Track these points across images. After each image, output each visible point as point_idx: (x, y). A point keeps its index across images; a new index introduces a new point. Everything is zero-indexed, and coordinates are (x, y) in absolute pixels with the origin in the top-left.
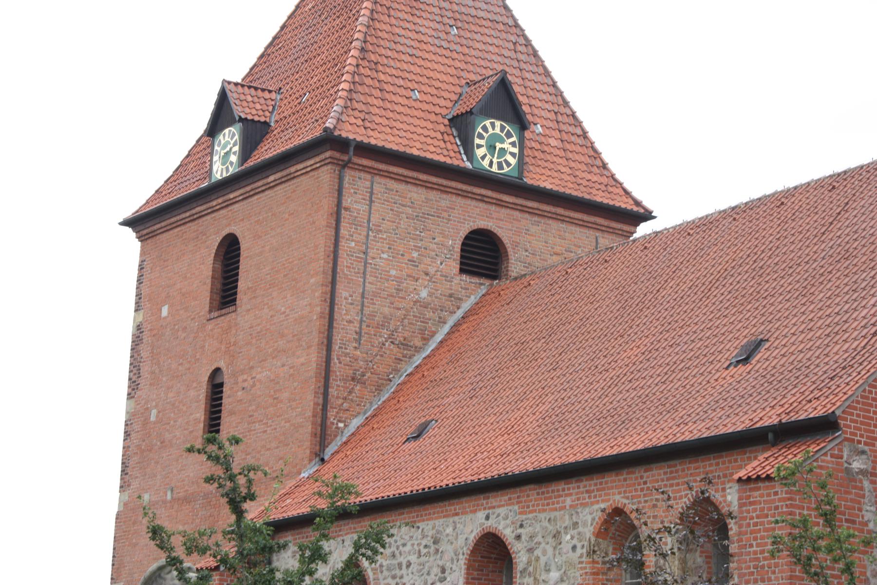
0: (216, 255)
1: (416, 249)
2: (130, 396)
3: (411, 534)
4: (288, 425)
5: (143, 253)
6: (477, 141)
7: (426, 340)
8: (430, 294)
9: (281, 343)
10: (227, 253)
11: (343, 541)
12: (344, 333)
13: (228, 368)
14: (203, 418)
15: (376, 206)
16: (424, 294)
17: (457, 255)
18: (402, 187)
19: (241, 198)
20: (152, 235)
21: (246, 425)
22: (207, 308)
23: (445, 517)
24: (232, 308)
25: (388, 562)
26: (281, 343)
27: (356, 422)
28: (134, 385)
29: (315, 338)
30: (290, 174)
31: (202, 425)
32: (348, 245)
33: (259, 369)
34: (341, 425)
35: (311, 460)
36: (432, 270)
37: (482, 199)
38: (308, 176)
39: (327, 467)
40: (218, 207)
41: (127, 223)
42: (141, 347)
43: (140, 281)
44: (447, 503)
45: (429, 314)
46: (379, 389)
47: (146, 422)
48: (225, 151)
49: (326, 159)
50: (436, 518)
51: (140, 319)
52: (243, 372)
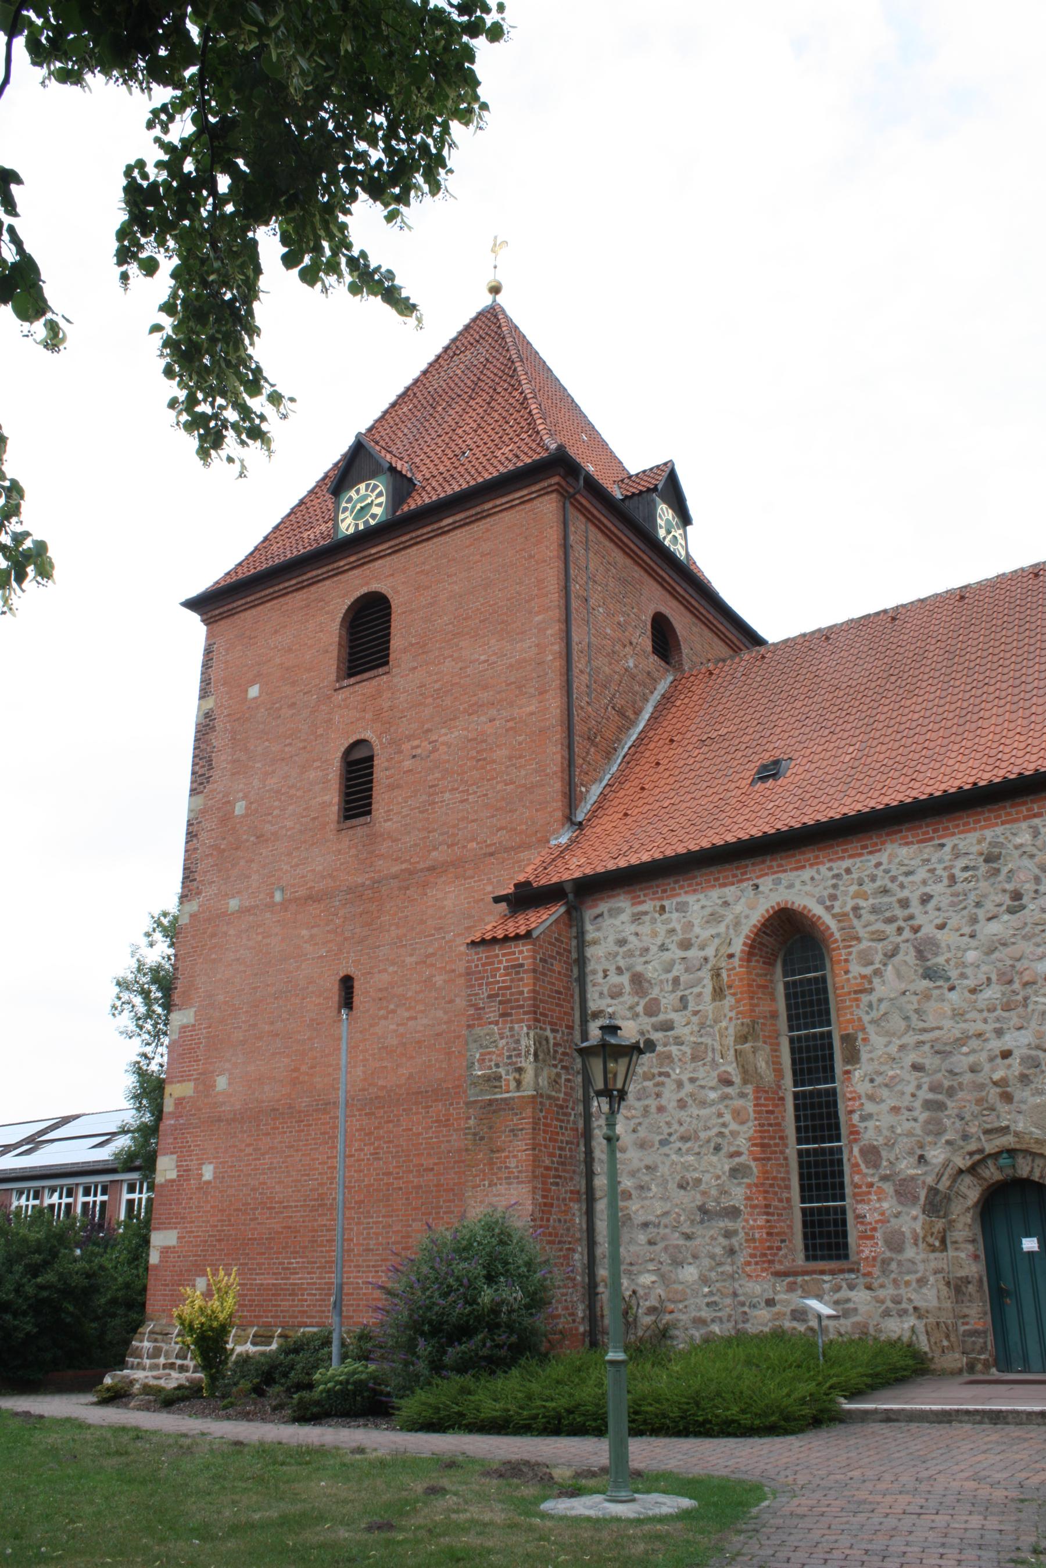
0: (344, 619)
1: (624, 614)
2: (194, 792)
3: (926, 856)
4: (509, 788)
5: (210, 636)
6: (659, 521)
7: (638, 713)
8: (636, 666)
9: (484, 696)
10: (353, 620)
11: (756, 887)
12: (580, 682)
13: (379, 737)
14: (336, 800)
15: (591, 555)
16: (631, 664)
17: (649, 633)
18: (607, 543)
19: (389, 551)
20: (222, 617)
21: (425, 797)
22: (333, 677)
23: (1003, 823)
24: (385, 669)
25: (871, 901)
26: (484, 696)
27: (596, 790)
28: (200, 781)
29: (555, 681)
30: (484, 511)
31: (335, 808)
32: (575, 588)
33: (443, 731)
34: (583, 789)
35: (563, 825)
36: (634, 641)
37: (661, 583)
38: (513, 511)
39: (588, 831)
40: (347, 567)
41: (193, 604)
42: (212, 736)
43: (206, 665)
44: (1008, 804)
45: (637, 688)
46: (609, 755)
47: (226, 818)
48: (363, 505)
49: (550, 486)
50: (982, 828)
51: (210, 703)
52: (409, 738)
